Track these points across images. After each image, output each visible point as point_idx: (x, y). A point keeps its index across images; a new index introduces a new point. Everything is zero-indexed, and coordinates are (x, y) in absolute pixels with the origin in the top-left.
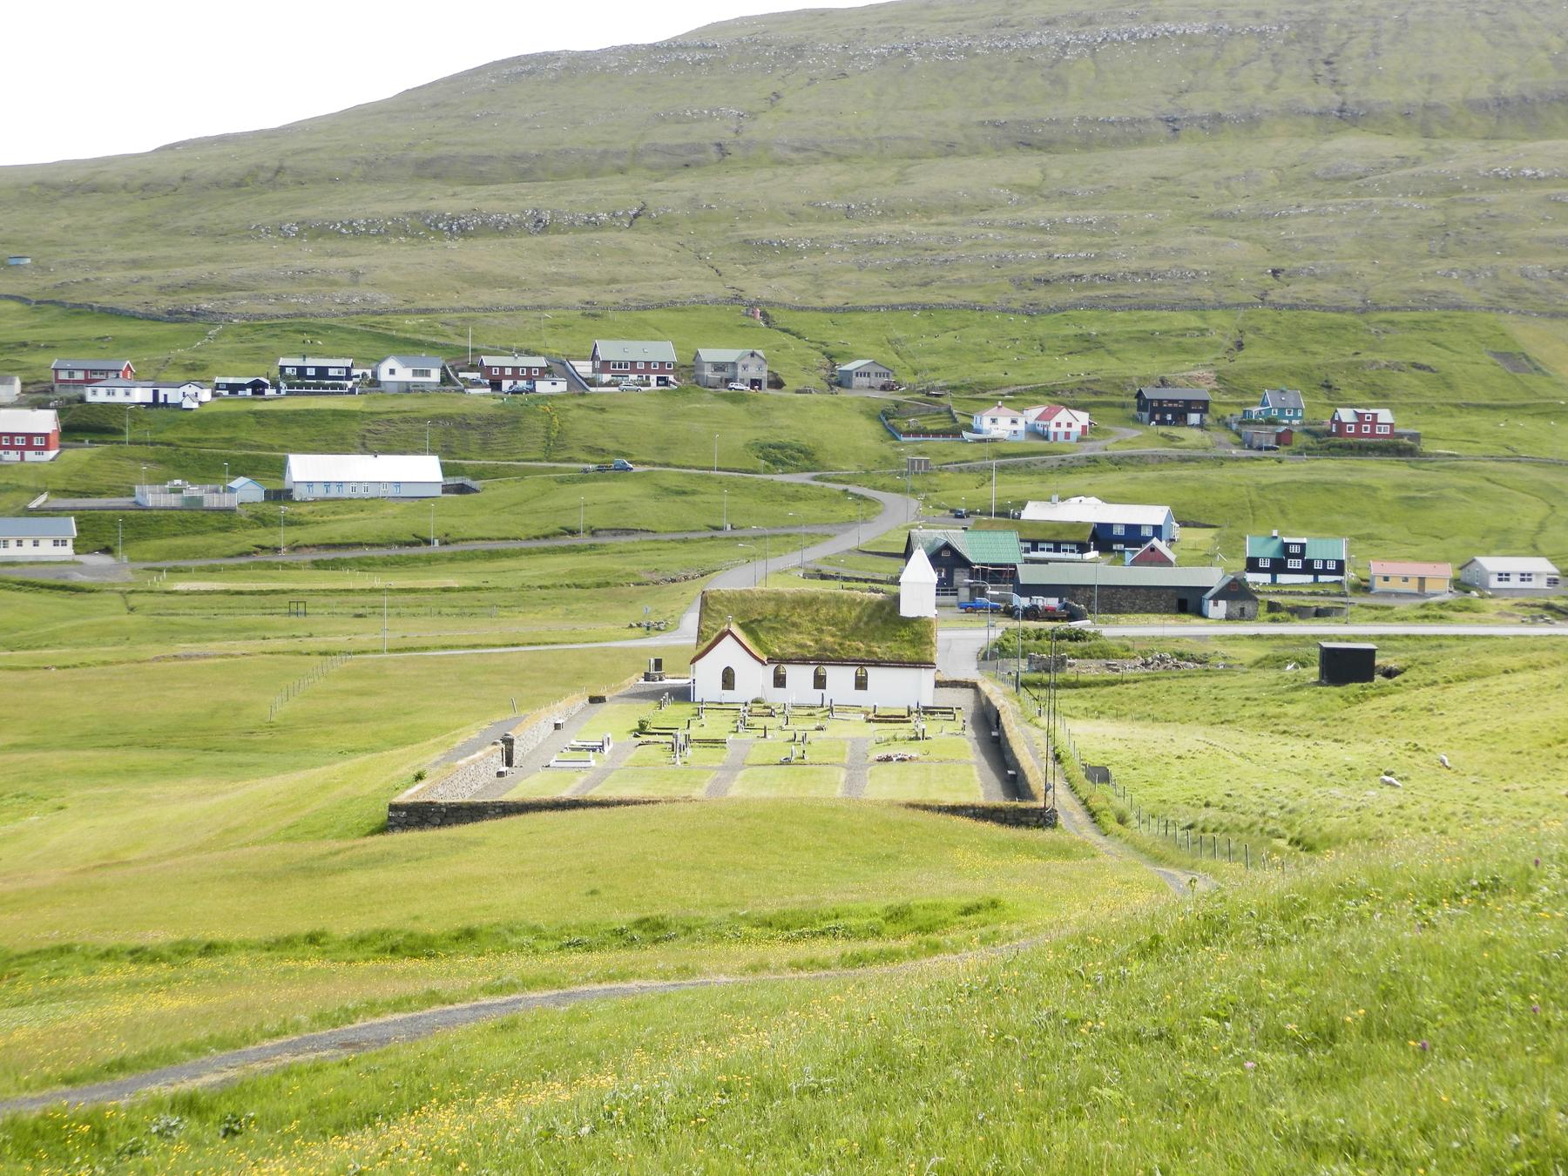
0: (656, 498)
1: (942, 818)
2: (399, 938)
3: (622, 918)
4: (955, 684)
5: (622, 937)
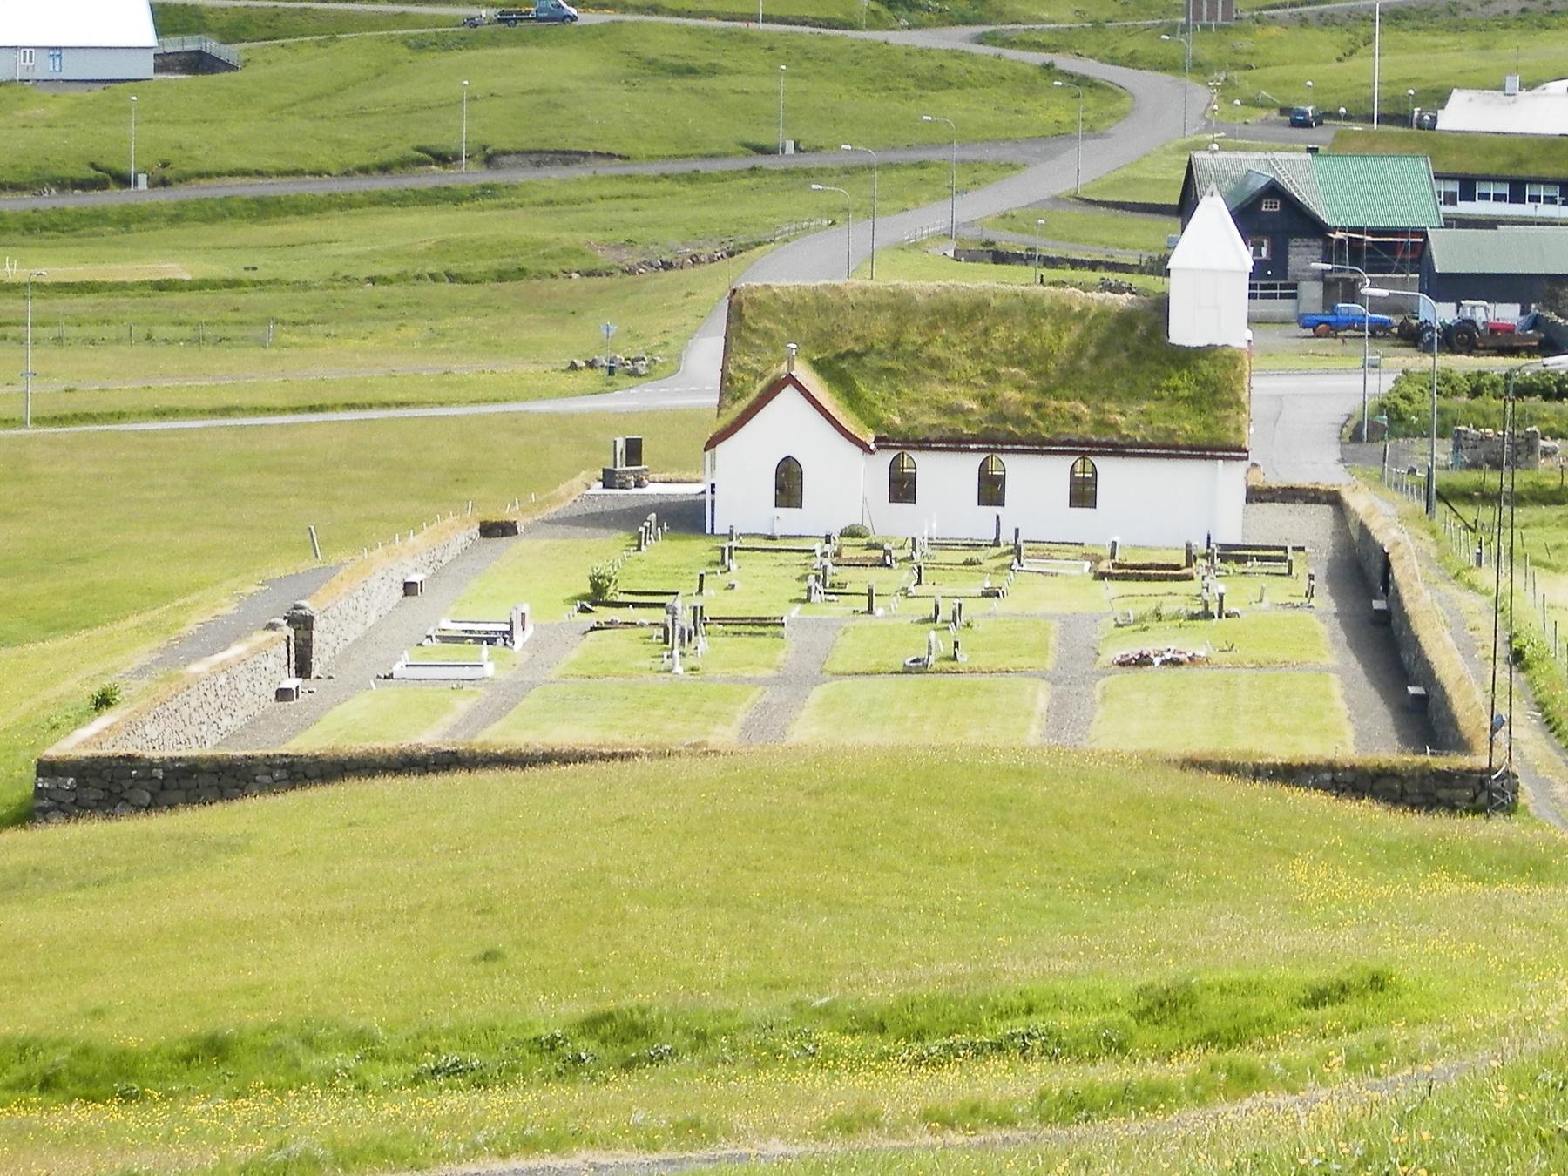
0: (628, 82)
1: (1265, 794)
2: (60, 1057)
3: (552, 1014)
4: (1290, 495)
5: (552, 1054)
